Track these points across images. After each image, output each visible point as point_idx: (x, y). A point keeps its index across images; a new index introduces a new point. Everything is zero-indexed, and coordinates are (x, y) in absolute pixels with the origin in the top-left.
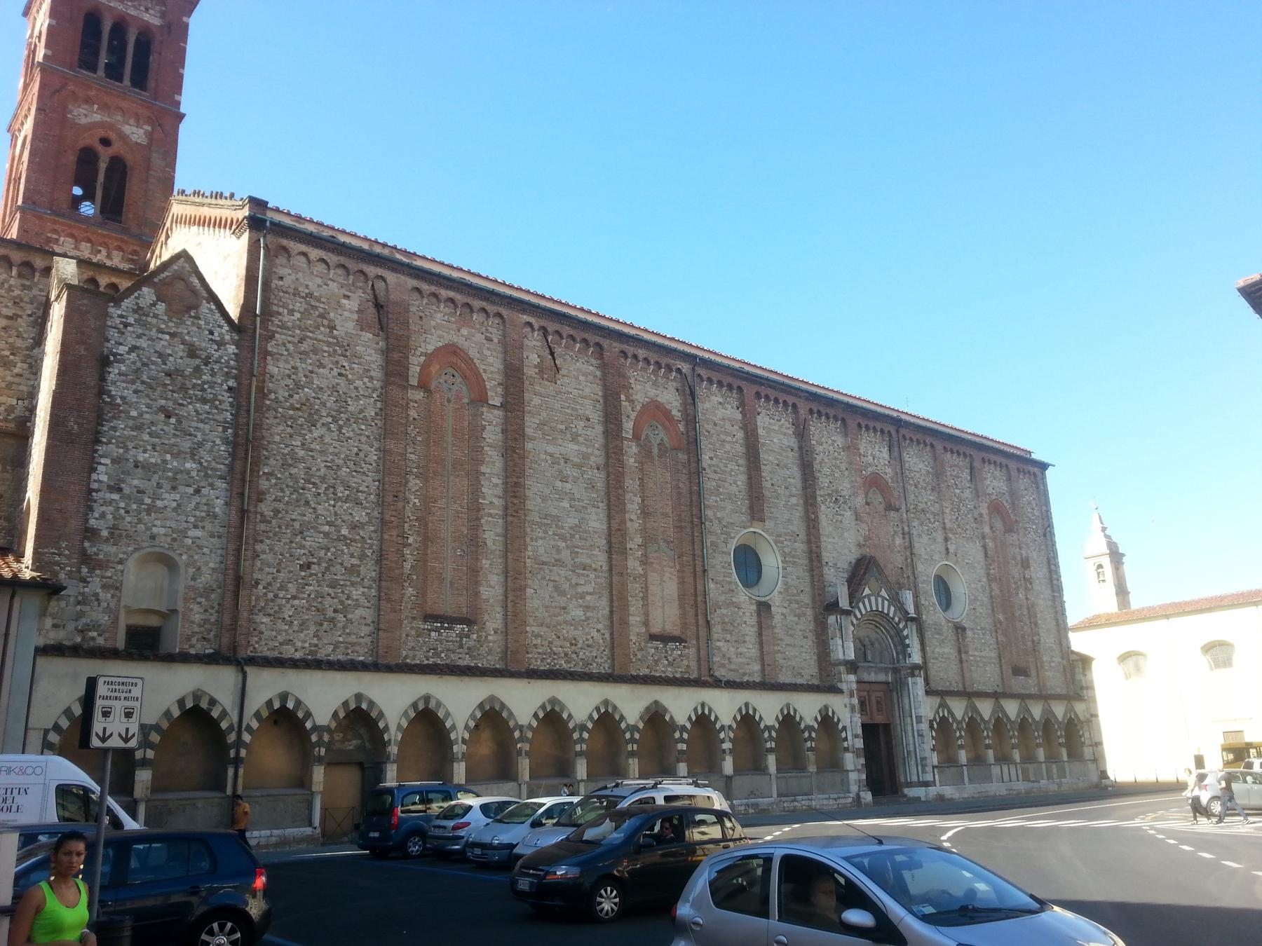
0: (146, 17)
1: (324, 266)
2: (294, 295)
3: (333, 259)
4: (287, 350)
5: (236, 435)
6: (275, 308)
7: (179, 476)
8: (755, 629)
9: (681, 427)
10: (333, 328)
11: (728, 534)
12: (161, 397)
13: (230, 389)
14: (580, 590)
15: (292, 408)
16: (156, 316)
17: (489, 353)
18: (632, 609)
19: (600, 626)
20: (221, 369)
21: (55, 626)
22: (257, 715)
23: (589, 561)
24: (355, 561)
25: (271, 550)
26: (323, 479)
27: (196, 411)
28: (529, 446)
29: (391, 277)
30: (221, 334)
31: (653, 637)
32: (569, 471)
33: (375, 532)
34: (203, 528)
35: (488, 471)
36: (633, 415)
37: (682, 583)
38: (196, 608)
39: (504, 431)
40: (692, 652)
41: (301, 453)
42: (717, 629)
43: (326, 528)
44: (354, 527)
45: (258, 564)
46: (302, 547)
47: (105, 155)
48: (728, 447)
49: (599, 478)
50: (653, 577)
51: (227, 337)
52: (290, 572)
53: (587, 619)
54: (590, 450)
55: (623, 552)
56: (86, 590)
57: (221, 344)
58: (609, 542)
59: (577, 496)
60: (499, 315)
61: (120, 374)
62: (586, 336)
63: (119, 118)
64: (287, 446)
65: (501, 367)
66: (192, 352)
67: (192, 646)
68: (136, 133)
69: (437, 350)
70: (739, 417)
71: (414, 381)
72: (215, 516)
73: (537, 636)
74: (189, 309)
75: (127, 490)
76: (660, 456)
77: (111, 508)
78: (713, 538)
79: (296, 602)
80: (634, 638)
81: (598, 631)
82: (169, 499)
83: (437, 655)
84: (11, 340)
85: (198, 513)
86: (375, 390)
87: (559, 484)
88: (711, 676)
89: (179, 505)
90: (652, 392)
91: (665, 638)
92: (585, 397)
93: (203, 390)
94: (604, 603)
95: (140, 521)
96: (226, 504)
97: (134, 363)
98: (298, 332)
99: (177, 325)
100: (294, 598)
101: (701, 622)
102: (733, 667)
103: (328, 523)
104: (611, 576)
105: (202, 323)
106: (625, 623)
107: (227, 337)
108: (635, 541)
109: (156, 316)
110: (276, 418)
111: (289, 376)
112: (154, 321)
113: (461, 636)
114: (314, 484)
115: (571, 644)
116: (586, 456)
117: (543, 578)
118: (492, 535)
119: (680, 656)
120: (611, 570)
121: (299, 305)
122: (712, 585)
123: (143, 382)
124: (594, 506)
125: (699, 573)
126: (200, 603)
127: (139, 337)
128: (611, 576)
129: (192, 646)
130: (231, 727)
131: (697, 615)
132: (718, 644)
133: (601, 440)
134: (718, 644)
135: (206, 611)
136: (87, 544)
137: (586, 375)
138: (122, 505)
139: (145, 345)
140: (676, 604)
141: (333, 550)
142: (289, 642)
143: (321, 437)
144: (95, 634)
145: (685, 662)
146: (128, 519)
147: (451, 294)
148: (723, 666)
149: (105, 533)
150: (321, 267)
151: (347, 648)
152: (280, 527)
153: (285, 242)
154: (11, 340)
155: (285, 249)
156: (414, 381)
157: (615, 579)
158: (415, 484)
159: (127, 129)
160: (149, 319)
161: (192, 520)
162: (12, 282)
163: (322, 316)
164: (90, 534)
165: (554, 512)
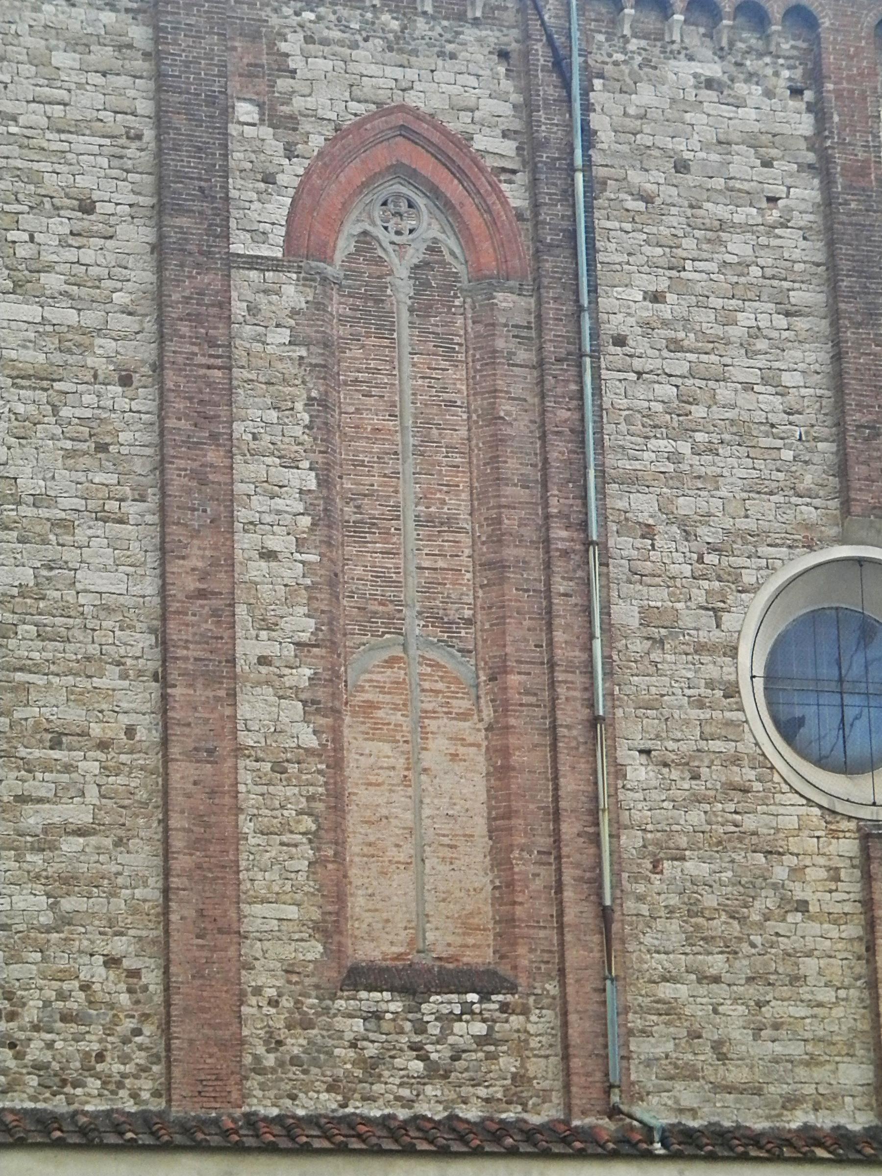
8: (853, 930)
9: (515, 195)
11: (733, 577)
14: (33, 819)
18: (259, 881)
19: (119, 946)
23: (74, 715)
31: (361, 977)
36: (290, 174)
37: (501, 770)
40: (540, 1023)
42: (655, 946)
48: (738, 246)
49: (130, 417)
50: (369, 756)
53: (65, 921)
54: (92, 318)
55: (222, 673)
58: (164, 643)
70: (805, 125)
76: (421, 310)
78: (658, 597)
80: (266, 979)
81: (111, 962)
88: (613, 1112)
90: (379, 74)
91: (411, 981)
92: (77, 128)
94: (141, 858)
101: (577, 909)
102: (737, 1075)
104: (166, 760)
106: (221, 927)
108: (274, 631)
116: (73, 342)
119: (481, 1041)
120: (165, 742)
122: (639, 772)
125: (572, 731)
128: (166, 760)
131: (559, 888)
132: (666, 991)
133: (142, 275)
134: (666, 991)
137: (79, 44)
140: (476, 856)
145: (508, 1063)
148: (691, 1074)
157: (182, 773)
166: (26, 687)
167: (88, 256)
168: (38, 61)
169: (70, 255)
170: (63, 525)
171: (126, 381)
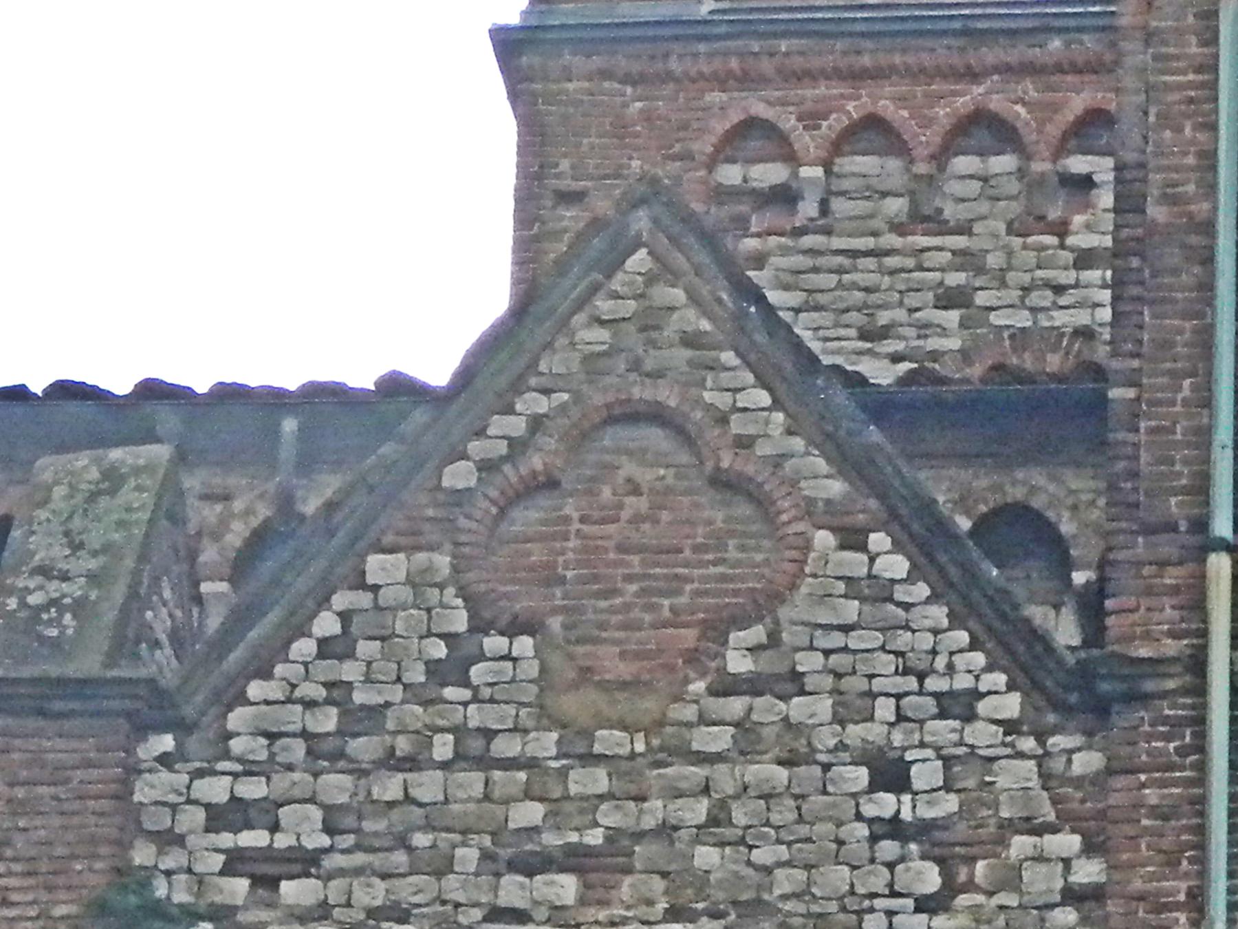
16: (475, 753)
74: (717, 630)
112: (472, 782)
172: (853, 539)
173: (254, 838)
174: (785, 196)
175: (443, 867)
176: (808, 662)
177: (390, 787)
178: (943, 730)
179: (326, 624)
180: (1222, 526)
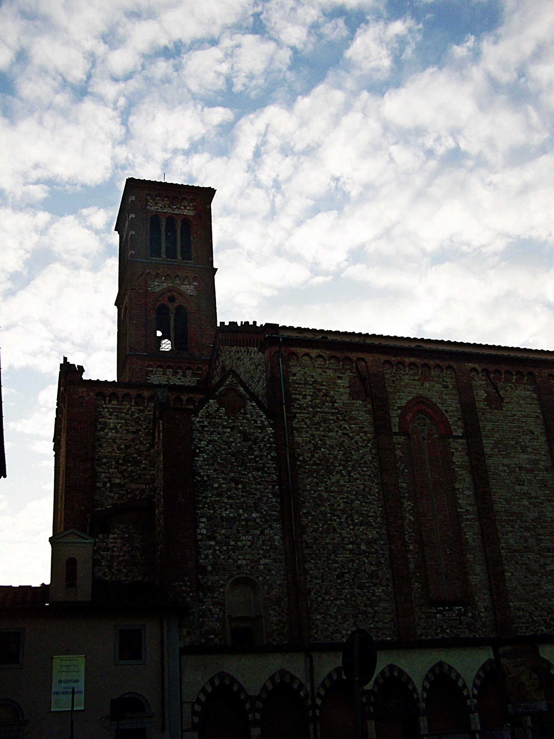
0: (186, 212)
1: (321, 359)
2: (305, 384)
3: (326, 353)
4: (306, 424)
5: (280, 489)
6: (294, 396)
7: (249, 523)
10: (333, 402)
12: (231, 471)
13: (273, 458)
15: (315, 464)
16: (220, 417)
17: (447, 397)
20: (265, 445)
21: (188, 633)
22: (323, 685)
24: (373, 568)
25: (316, 567)
26: (343, 511)
27: (254, 477)
28: (489, 462)
29: (368, 357)
30: (262, 422)
32: (524, 476)
33: (384, 544)
34: (269, 556)
35: (461, 486)
38: (272, 612)
39: (469, 454)
41: (325, 495)
43: (350, 546)
44: (369, 543)
45: (308, 577)
46: (336, 562)
47: (172, 307)
51: (266, 423)
52: (330, 581)
54: (538, 457)
56: (204, 607)
57: (263, 428)
59: (534, 494)
60: (449, 367)
61: (204, 460)
62: (520, 369)
63: (179, 282)
64: (315, 491)
65: (459, 406)
66: (246, 437)
67: (274, 640)
68: (189, 289)
69: (409, 402)
71: (396, 430)
72: (276, 548)
73: (519, 609)
75: (219, 537)
77: (210, 551)
79: (338, 602)
82: (246, 540)
83: (443, 631)
84: (137, 447)
85: (264, 547)
86: (369, 441)
87: (517, 487)
89: (252, 543)
92: (527, 416)
93: (256, 462)
95: (230, 557)
96: (282, 538)
97: (211, 451)
98: (311, 409)
99: (234, 421)
100: (336, 599)
103: (351, 543)
105: (248, 416)
107: (266, 423)
109: (220, 417)
110: (305, 473)
111: (310, 442)
112: (220, 421)
113: (460, 614)
114: (338, 516)
115: (548, 613)
116: (536, 462)
117: (517, 563)
118: (471, 536)
121: (309, 391)
123: (218, 463)
124: (549, 501)
126: (274, 609)
127: (212, 433)
129: (274, 640)
130: (307, 695)
135: (279, 614)
136: (200, 577)
138: (217, 548)
139: (216, 438)
141: (357, 561)
142: (337, 631)
143: (338, 481)
144: (213, 636)
146: (222, 557)
147: (413, 360)
149: (209, 568)
150: (320, 361)
151: (377, 632)
152: (319, 550)
153: (293, 349)
154: (137, 447)
155: (294, 354)
156: (396, 430)
158: (408, 504)
159: (183, 288)
160: (217, 420)
161: (262, 552)
162: (133, 409)
163: (325, 395)
164: (202, 570)
165: (516, 509)
166: (541, 539)
167: (535, 444)
168: (518, 403)
169: (531, 444)
170: (542, 503)
171: (547, 470)
172: (251, 402)
173: (201, 424)
174: (152, 371)
175: (218, 428)
176: (248, 412)
177: (213, 420)
178: (260, 418)
179: (206, 406)
180: (284, 402)
